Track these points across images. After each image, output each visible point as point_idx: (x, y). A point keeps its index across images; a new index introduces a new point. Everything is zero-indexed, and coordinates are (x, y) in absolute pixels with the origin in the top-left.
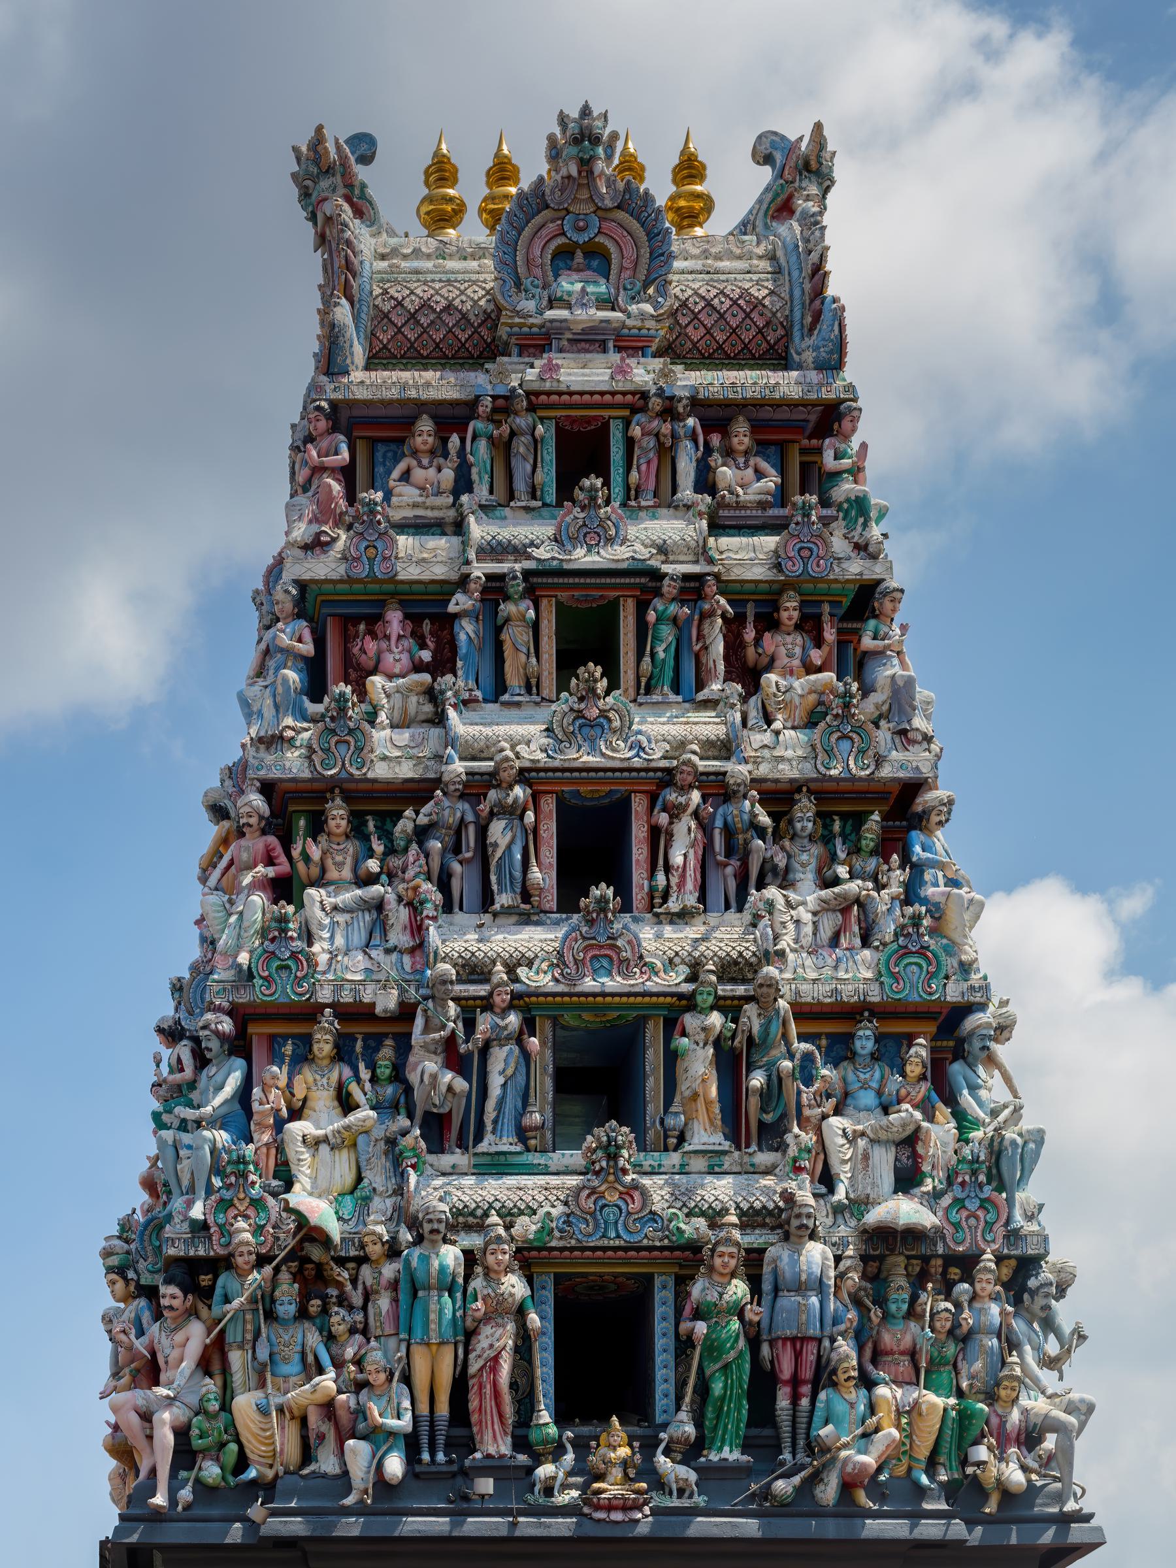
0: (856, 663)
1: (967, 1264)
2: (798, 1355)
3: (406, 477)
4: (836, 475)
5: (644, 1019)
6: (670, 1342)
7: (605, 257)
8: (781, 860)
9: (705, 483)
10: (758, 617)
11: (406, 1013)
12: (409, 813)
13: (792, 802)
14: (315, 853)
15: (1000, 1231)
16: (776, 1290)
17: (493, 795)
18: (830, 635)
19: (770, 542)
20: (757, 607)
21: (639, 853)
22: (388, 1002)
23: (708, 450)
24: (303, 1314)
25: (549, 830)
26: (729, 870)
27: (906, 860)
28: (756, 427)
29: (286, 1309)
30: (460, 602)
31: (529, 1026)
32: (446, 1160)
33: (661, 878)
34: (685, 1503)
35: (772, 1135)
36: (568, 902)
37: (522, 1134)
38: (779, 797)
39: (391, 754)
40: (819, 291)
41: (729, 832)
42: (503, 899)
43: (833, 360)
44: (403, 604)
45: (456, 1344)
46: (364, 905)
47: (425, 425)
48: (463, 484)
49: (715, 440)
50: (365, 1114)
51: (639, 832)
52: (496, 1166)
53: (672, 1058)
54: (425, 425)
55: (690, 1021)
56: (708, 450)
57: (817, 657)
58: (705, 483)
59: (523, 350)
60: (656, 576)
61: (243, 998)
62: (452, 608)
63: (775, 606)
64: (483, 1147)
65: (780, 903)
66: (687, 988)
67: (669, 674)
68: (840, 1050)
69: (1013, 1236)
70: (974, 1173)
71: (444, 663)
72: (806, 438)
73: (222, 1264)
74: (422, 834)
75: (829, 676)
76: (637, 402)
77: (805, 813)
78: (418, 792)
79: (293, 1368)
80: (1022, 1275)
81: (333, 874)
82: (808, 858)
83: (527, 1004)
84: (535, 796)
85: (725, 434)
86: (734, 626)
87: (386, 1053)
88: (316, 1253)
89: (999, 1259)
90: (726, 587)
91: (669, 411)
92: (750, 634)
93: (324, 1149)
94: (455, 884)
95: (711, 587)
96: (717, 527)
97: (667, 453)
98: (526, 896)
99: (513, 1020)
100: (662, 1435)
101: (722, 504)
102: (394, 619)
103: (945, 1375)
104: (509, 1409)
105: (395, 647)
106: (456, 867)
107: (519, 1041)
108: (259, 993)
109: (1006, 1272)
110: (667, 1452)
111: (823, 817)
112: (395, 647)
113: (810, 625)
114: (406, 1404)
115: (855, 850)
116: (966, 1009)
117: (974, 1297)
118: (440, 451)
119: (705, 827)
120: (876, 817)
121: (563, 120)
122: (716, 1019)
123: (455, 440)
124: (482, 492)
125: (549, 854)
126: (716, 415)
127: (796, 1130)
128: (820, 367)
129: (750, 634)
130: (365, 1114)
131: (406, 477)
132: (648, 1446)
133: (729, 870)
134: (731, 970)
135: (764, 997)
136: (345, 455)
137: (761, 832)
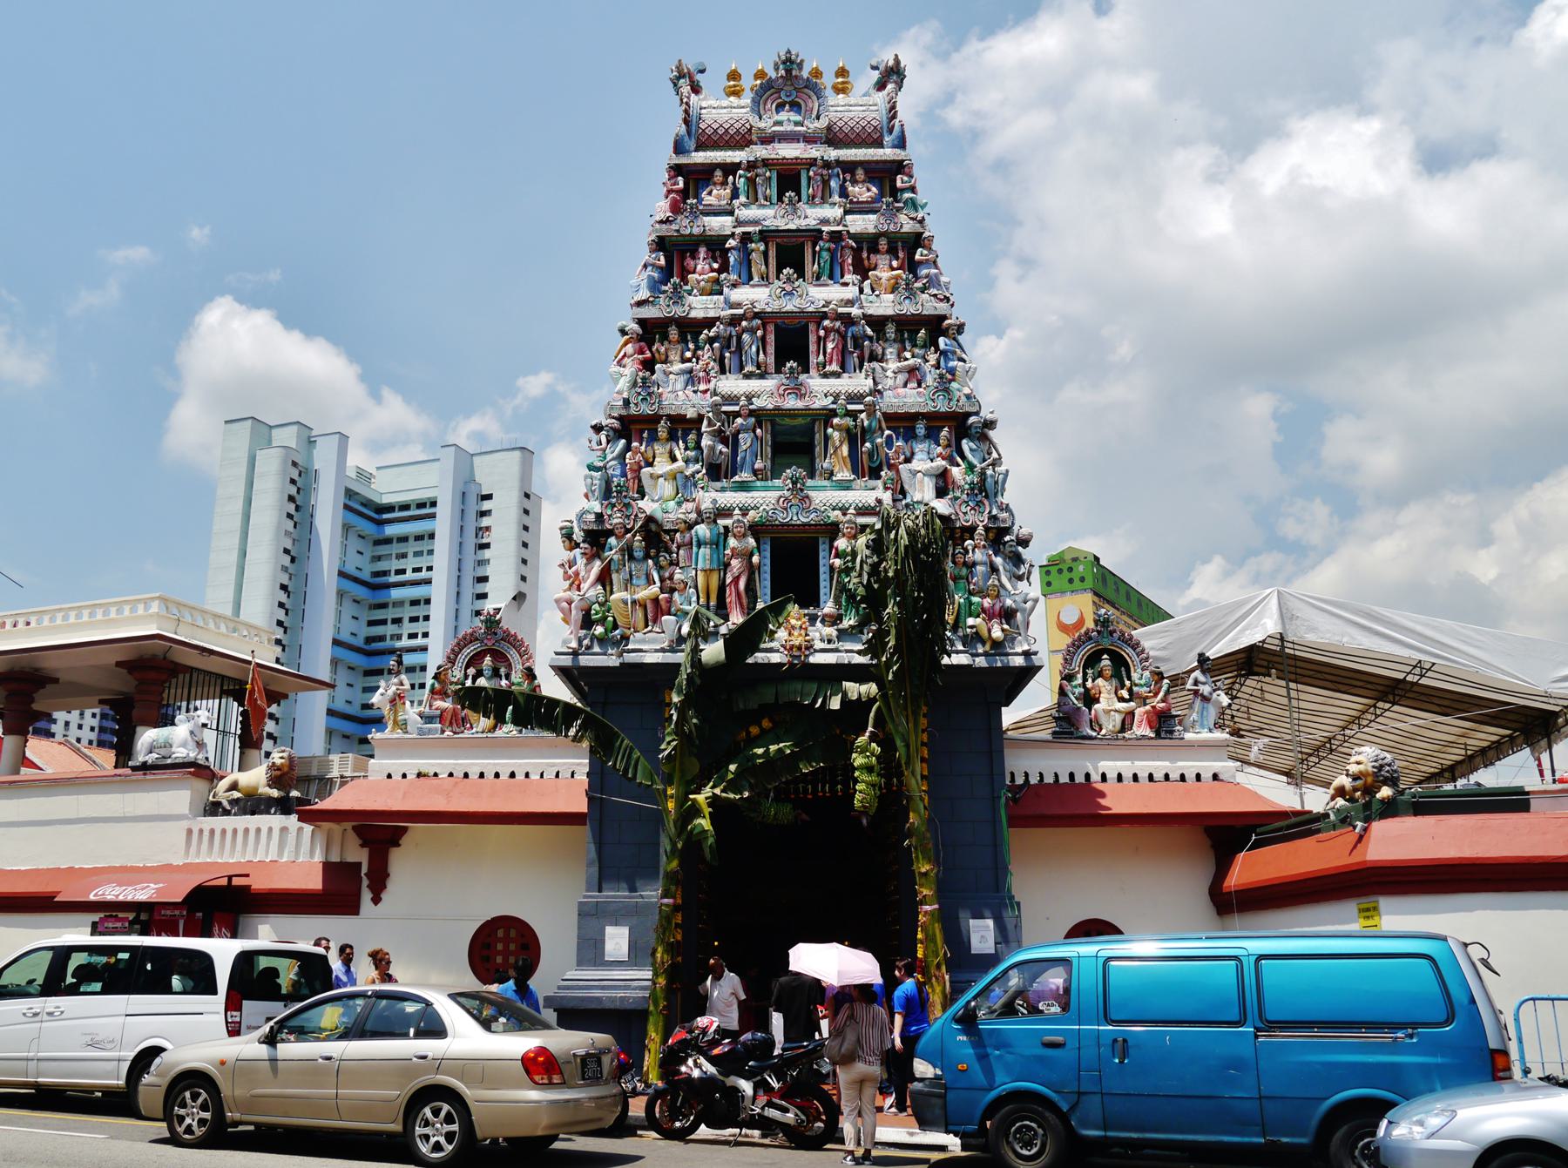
0: (912, 266)
1: (970, 531)
3: (710, 193)
4: (903, 190)
5: (814, 422)
6: (827, 569)
7: (799, 106)
9: (844, 193)
11: (700, 418)
14: (663, 349)
15: (986, 515)
17: (744, 323)
18: (901, 255)
19: (873, 217)
20: (869, 243)
21: (812, 348)
22: (691, 413)
23: (845, 180)
25: (771, 338)
27: (937, 349)
28: (867, 172)
29: (638, 554)
30: (731, 243)
31: (759, 424)
32: (718, 485)
33: (821, 357)
34: (831, 646)
35: (875, 474)
36: (778, 371)
37: (755, 472)
38: (878, 323)
39: (700, 306)
40: (894, 117)
41: (854, 338)
42: (749, 368)
43: (901, 143)
44: (707, 245)
46: (683, 372)
47: (718, 174)
48: (735, 194)
50: (680, 464)
51: (812, 338)
52: (743, 487)
53: (827, 438)
54: (718, 174)
55: (836, 421)
56: (845, 180)
57: (895, 264)
58: (844, 193)
59: (763, 143)
60: (821, 232)
63: (877, 244)
64: (736, 478)
65: (879, 369)
67: (827, 272)
68: (910, 435)
69: (993, 518)
70: (972, 489)
71: (724, 268)
72: (887, 176)
73: (610, 533)
74: (711, 341)
76: (812, 162)
78: (709, 323)
79: (643, 581)
80: (997, 536)
81: (672, 357)
82: (891, 352)
83: (760, 416)
85: (853, 175)
86: (856, 253)
87: (692, 437)
88: (653, 527)
89: (987, 529)
92: (865, 255)
97: (826, 183)
98: (759, 367)
99: (752, 420)
101: (851, 202)
102: (702, 251)
103: (962, 583)
104: (745, 601)
108: (633, 410)
109: (991, 535)
110: (823, 622)
111: (899, 331)
112: (703, 268)
113: (892, 251)
114: (694, 599)
115: (915, 345)
116: (969, 415)
117: (975, 547)
118: (724, 183)
119: (844, 337)
122: (849, 421)
123: (731, 178)
124: (743, 199)
125: (771, 349)
126: (849, 167)
128: (894, 147)
129: (865, 255)
130: (680, 464)
131: (710, 193)
132: (813, 619)
134: (855, 398)
135: (871, 410)
136: (681, 185)
137: (870, 339)
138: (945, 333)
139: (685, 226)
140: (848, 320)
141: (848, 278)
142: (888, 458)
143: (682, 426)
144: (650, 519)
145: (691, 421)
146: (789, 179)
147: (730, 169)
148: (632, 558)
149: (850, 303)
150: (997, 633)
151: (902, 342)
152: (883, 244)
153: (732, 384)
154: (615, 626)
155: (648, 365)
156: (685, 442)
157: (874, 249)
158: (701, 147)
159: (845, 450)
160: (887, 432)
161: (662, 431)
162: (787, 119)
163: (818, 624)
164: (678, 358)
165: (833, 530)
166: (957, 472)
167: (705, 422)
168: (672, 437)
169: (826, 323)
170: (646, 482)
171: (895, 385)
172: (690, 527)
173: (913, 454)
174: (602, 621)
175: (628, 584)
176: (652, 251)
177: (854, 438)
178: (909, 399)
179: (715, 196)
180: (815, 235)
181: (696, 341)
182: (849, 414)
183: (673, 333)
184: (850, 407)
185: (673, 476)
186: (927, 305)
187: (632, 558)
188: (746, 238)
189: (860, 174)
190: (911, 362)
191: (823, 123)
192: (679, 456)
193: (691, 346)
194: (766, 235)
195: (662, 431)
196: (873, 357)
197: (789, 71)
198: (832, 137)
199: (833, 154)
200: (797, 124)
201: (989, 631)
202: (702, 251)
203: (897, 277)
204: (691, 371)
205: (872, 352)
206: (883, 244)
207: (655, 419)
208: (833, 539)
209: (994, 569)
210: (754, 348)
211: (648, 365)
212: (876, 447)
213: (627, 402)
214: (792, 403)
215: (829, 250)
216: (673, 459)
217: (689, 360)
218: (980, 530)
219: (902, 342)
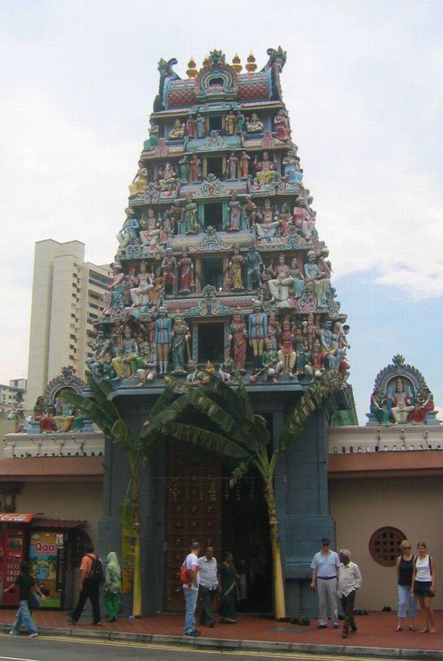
1: (307, 315)
2: (258, 343)
8: (261, 216)
9: (245, 128)
10: (257, 159)
12: (167, 211)
13: (264, 202)
16: (252, 327)
18: (275, 161)
20: (256, 155)
22: (158, 257)
24: (132, 337)
26: (248, 220)
29: (128, 336)
38: (259, 201)
45: (169, 343)
47: (177, 122)
49: (247, 118)
54: (177, 122)
56: (246, 121)
61: (123, 258)
62: (180, 162)
66: (232, 250)
73: (113, 325)
75: (274, 171)
76: (227, 112)
77: (268, 206)
78: (168, 206)
83: (193, 257)
84: (198, 205)
85: (251, 117)
86: (250, 162)
90: (248, 153)
91: (235, 113)
92: (255, 162)
93: (141, 295)
94: (179, 227)
95: (244, 153)
96: (247, 139)
100: (221, 365)
105: (169, 173)
106: (179, 223)
107: (190, 265)
108: (128, 257)
109: (318, 318)
112: (169, 173)
120: (285, 204)
121: (211, 53)
123: (184, 124)
126: (248, 114)
127: (260, 284)
132: (217, 368)
133: (248, 220)
135: (252, 250)
138: (297, 204)
139: (156, 153)
140: (243, 201)
141: (246, 176)
142: (261, 278)
143: (152, 264)
144: (133, 317)
145: (157, 261)
146: (216, 122)
147: (183, 119)
148: (124, 337)
149: (243, 191)
150: (318, 373)
151: (274, 210)
152: (265, 155)
153: (181, 241)
154: (115, 375)
155: (137, 231)
156: (155, 273)
157: (261, 159)
158: (171, 106)
159: (239, 273)
160: (261, 263)
161: (143, 268)
162: (217, 90)
163: (220, 371)
164: (153, 226)
165: (230, 318)
166: (300, 283)
167: (164, 262)
168: (148, 270)
169: (231, 203)
170: (133, 295)
171: (268, 236)
172: (154, 319)
173: (278, 273)
174: (108, 373)
175: (123, 352)
176: (141, 168)
177: (244, 267)
178: (278, 243)
179: (174, 133)
180: (228, 153)
181: (162, 217)
182: (241, 253)
183: (151, 213)
184: (242, 250)
185: (147, 292)
186: (289, 189)
187: (124, 337)
188: (190, 157)
189: (255, 117)
190: (277, 222)
191: (235, 89)
192: (151, 281)
193: (160, 219)
194: (200, 155)
195: (143, 268)
196: (259, 221)
197: (216, 62)
198: (242, 97)
199: (238, 107)
200: (220, 91)
201: (314, 371)
202: (168, 166)
203: (272, 174)
204: (158, 234)
205: (257, 217)
206: (265, 155)
207: (139, 261)
208: (230, 323)
209: (318, 337)
210: (192, 220)
211: (137, 231)
212: (255, 271)
213: (124, 253)
214: (211, 248)
215: (234, 161)
216: (149, 282)
217: (159, 228)
218: (311, 316)
219: (274, 210)
